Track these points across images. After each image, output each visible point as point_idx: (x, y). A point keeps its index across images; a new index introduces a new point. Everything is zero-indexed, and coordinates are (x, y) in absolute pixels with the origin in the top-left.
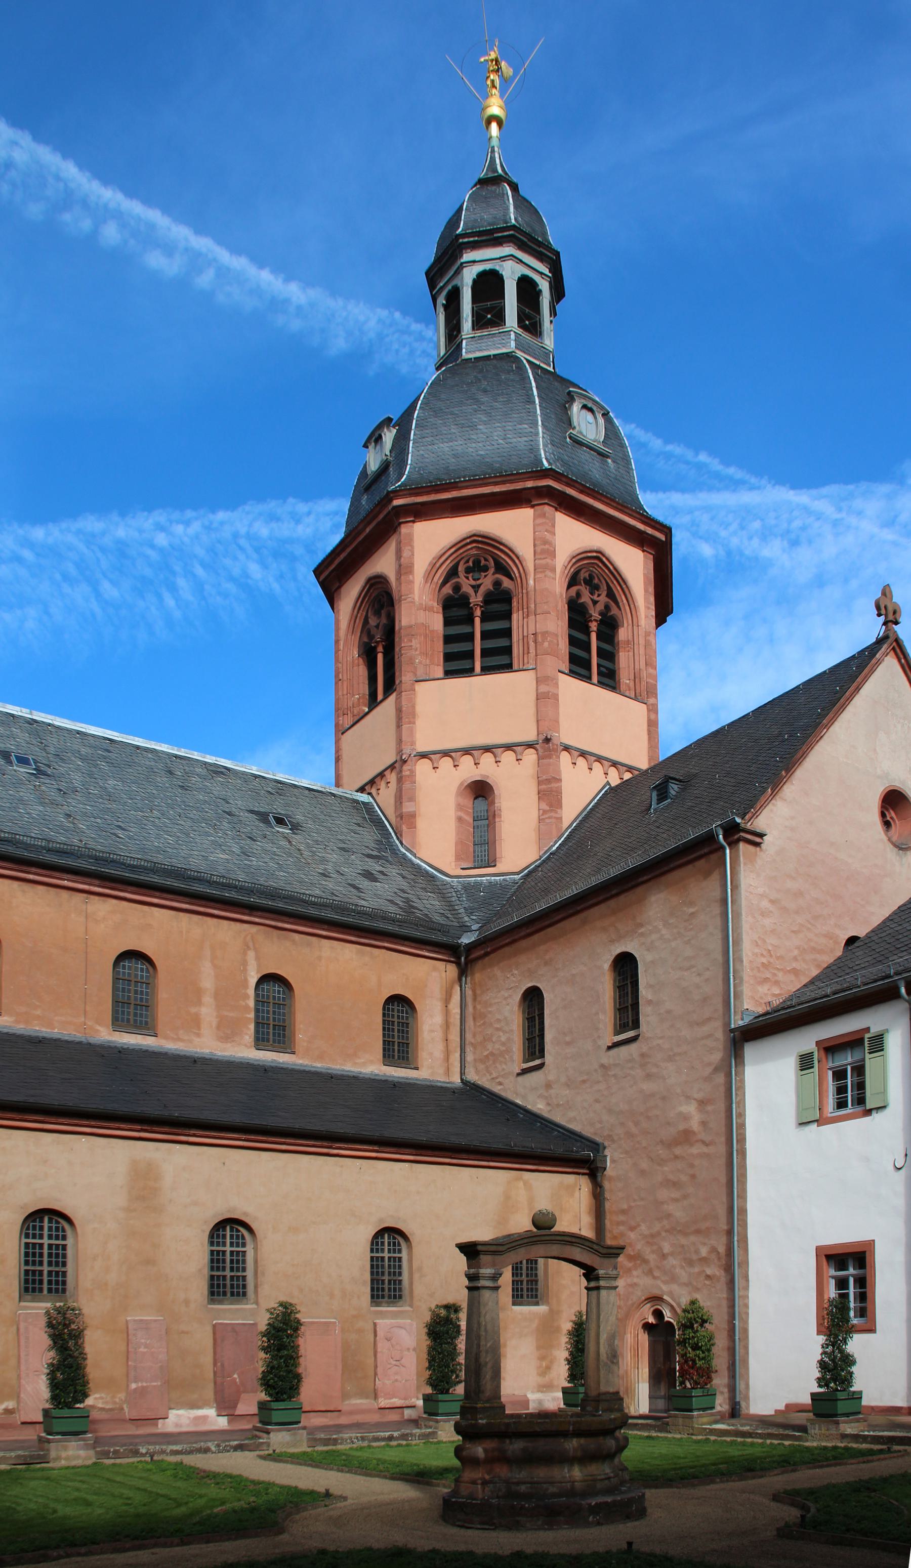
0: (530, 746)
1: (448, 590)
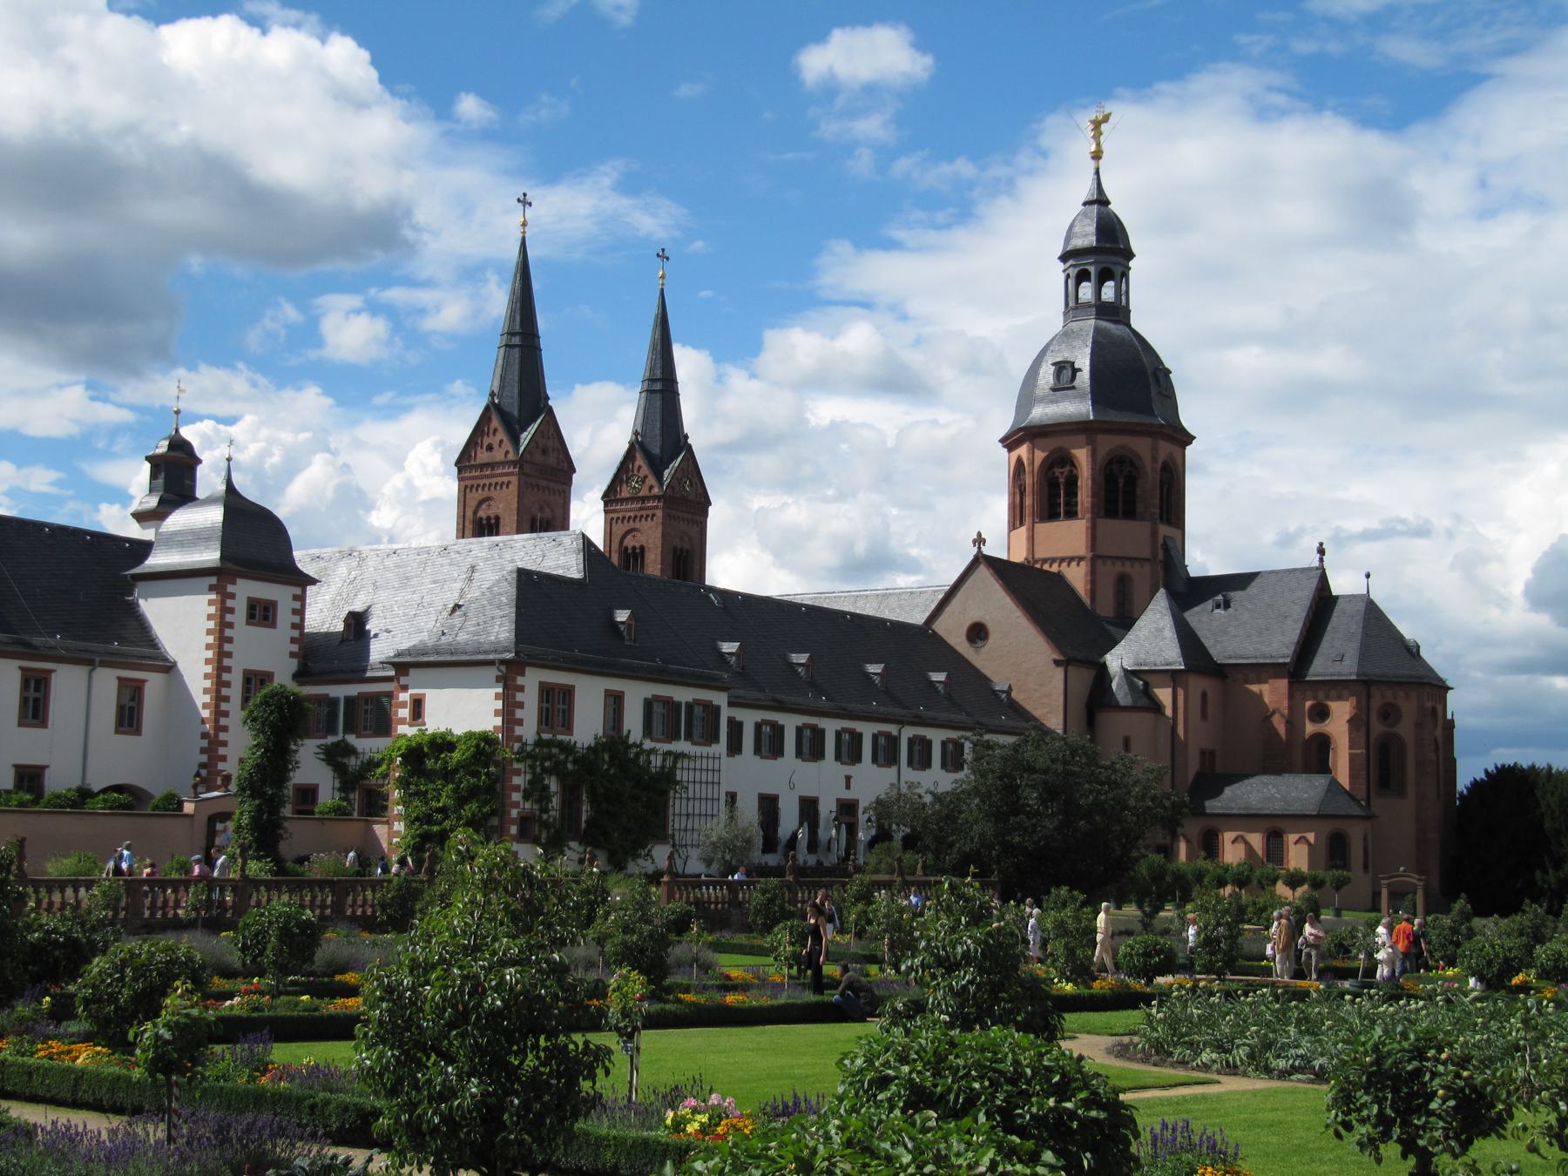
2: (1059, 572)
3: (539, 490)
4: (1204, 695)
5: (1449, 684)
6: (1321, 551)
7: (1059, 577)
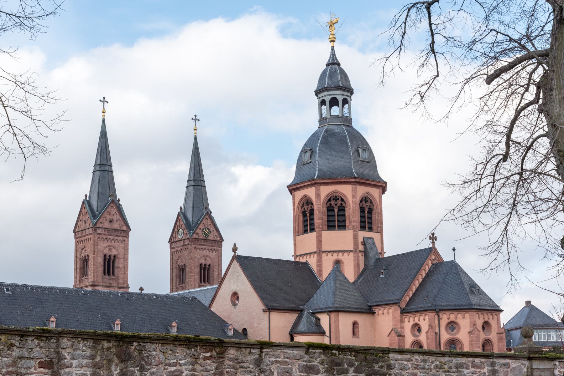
0: (351, 251)
1: (328, 205)
3: (108, 241)
4: (355, 324)
5: (502, 308)
6: (433, 238)
7: (306, 264)
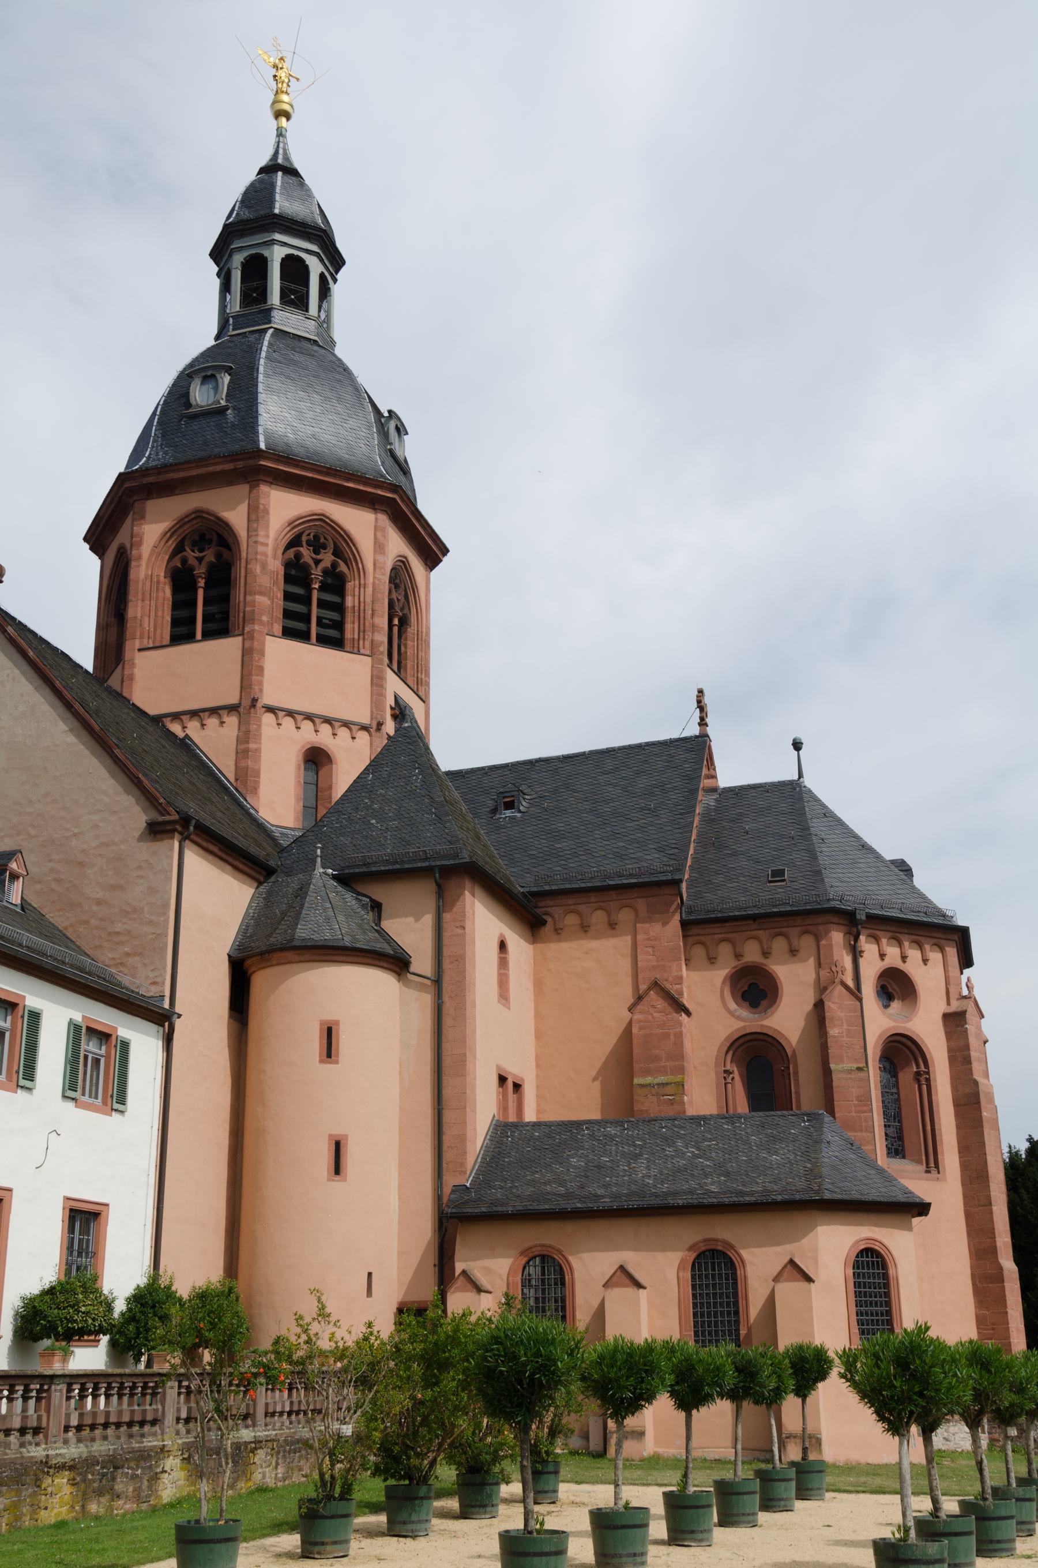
0: (364, 728)
2: (187, 736)
7: (185, 745)
